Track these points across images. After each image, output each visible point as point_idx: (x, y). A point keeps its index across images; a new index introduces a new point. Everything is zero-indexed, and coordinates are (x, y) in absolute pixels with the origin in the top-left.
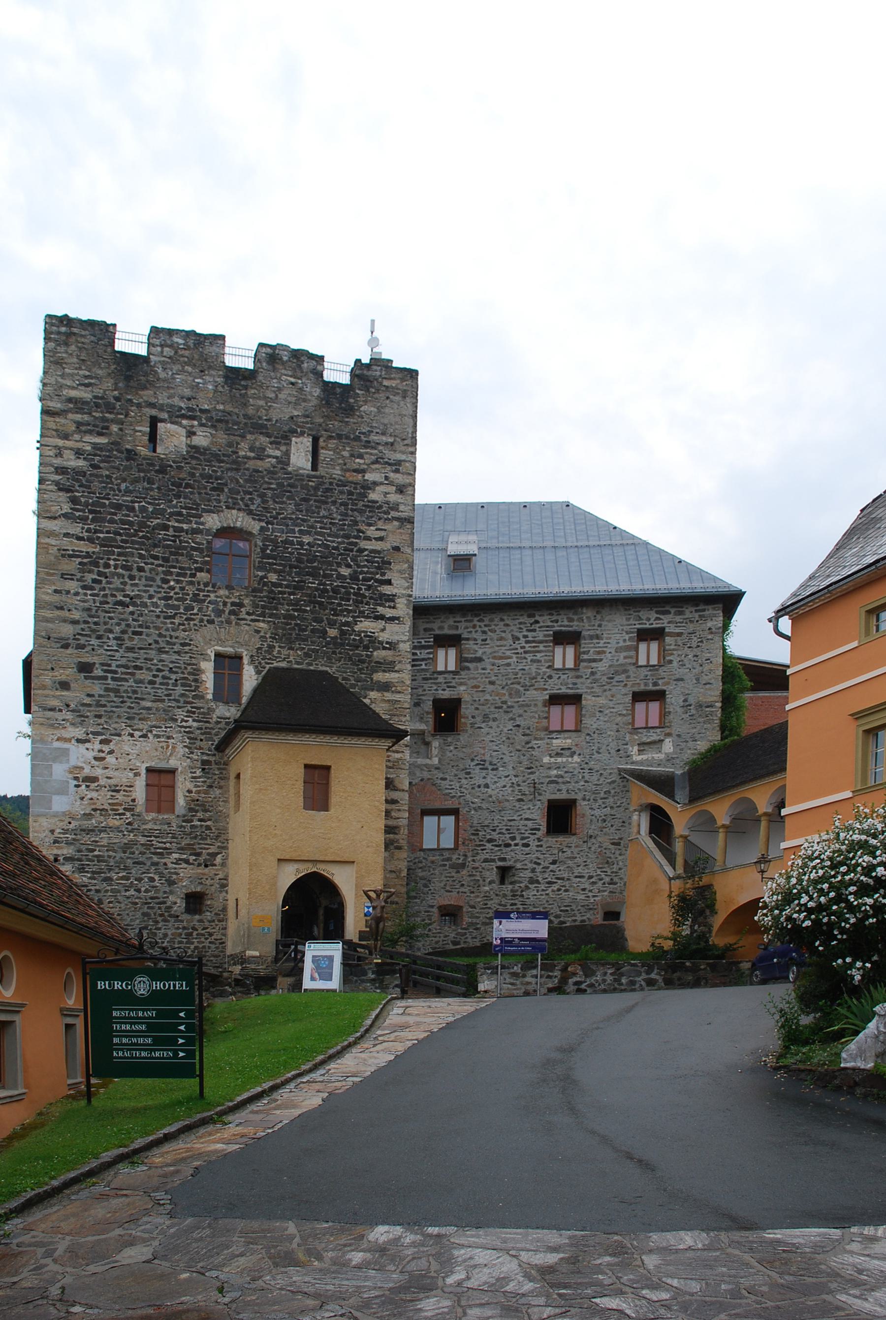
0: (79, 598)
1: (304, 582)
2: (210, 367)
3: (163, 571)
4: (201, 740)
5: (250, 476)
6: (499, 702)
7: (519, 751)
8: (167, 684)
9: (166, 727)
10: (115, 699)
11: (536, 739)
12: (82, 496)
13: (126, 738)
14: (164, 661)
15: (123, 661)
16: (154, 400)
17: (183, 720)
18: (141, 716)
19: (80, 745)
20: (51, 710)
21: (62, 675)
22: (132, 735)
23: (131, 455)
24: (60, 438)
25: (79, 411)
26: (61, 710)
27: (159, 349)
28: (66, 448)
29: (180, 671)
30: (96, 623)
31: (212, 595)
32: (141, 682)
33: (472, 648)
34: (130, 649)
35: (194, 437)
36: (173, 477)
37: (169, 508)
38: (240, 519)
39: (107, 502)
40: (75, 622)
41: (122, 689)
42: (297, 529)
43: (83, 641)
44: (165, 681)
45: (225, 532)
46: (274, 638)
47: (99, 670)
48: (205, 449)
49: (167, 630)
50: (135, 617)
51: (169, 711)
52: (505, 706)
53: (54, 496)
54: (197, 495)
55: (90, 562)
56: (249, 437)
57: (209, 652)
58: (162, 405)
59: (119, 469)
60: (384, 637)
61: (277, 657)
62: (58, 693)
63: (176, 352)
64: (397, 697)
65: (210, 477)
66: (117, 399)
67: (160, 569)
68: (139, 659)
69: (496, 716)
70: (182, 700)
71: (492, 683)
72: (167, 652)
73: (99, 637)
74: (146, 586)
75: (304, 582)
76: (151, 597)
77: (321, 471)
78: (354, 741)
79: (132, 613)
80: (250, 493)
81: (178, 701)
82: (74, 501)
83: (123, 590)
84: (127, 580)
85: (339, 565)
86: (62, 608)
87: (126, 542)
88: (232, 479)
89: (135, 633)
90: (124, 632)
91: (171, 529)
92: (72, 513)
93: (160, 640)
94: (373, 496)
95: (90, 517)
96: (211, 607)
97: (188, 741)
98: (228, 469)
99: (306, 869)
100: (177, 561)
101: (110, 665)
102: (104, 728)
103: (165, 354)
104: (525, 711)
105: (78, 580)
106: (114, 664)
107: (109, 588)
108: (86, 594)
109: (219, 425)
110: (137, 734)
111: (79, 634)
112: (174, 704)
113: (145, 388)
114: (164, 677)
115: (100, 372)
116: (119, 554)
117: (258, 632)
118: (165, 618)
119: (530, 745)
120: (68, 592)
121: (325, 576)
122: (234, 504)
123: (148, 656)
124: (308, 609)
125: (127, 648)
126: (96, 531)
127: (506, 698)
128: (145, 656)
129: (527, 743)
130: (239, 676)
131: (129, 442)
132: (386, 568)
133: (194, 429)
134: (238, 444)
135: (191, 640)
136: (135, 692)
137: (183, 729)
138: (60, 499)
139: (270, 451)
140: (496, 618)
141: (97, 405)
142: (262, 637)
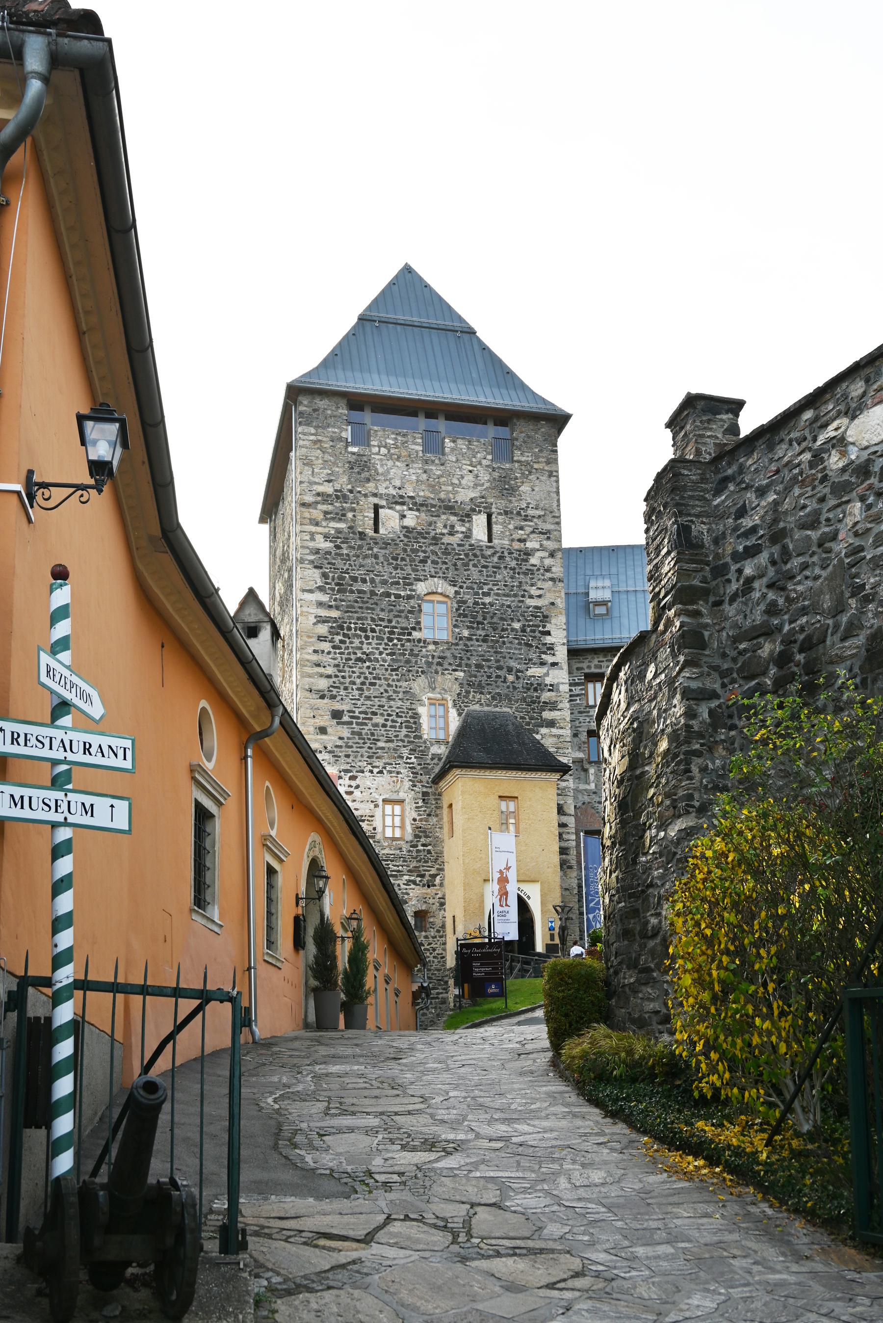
2: (413, 461)
3: (389, 632)
5: (446, 549)
8: (395, 727)
13: (368, 774)
15: (363, 708)
17: (407, 758)
22: (371, 772)
23: (362, 536)
24: (313, 525)
25: (325, 502)
27: (377, 449)
30: (343, 677)
31: (424, 650)
32: (376, 725)
34: (368, 698)
35: (405, 520)
37: (390, 578)
40: (329, 677)
41: (364, 732)
42: (480, 591)
46: (469, 685)
49: (393, 680)
50: (370, 670)
55: (338, 627)
56: (444, 517)
57: (423, 698)
58: (381, 494)
59: (354, 548)
60: (548, 681)
62: (319, 737)
63: (389, 451)
64: (560, 732)
65: (418, 551)
66: (351, 491)
67: (386, 629)
70: (406, 740)
72: (394, 700)
73: (346, 689)
74: (377, 644)
75: (488, 636)
76: (381, 653)
77: (496, 542)
78: (533, 775)
79: (368, 667)
80: (446, 563)
82: (325, 576)
83: (361, 648)
84: (364, 640)
85: (512, 620)
86: (318, 665)
87: (361, 608)
90: (363, 683)
91: (393, 597)
93: (389, 689)
94: (533, 560)
96: (424, 659)
100: (398, 622)
101: (354, 712)
105: (330, 642)
106: (357, 710)
108: (335, 653)
110: (376, 770)
111: (332, 686)
112: (400, 744)
113: (368, 480)
114: (393, 721)
115: (337, 469)
116: (358, 619)
117: (456, 679)
118: (392, 670)
120: (323, 652)
121: (503, 630)
123: (381, 703)
125: (366, 697)
130: (446, 717)
133: (405, 513)
136: (373, 734)
139: (458, 528)
141: (337, 497)
142: (461, 684)
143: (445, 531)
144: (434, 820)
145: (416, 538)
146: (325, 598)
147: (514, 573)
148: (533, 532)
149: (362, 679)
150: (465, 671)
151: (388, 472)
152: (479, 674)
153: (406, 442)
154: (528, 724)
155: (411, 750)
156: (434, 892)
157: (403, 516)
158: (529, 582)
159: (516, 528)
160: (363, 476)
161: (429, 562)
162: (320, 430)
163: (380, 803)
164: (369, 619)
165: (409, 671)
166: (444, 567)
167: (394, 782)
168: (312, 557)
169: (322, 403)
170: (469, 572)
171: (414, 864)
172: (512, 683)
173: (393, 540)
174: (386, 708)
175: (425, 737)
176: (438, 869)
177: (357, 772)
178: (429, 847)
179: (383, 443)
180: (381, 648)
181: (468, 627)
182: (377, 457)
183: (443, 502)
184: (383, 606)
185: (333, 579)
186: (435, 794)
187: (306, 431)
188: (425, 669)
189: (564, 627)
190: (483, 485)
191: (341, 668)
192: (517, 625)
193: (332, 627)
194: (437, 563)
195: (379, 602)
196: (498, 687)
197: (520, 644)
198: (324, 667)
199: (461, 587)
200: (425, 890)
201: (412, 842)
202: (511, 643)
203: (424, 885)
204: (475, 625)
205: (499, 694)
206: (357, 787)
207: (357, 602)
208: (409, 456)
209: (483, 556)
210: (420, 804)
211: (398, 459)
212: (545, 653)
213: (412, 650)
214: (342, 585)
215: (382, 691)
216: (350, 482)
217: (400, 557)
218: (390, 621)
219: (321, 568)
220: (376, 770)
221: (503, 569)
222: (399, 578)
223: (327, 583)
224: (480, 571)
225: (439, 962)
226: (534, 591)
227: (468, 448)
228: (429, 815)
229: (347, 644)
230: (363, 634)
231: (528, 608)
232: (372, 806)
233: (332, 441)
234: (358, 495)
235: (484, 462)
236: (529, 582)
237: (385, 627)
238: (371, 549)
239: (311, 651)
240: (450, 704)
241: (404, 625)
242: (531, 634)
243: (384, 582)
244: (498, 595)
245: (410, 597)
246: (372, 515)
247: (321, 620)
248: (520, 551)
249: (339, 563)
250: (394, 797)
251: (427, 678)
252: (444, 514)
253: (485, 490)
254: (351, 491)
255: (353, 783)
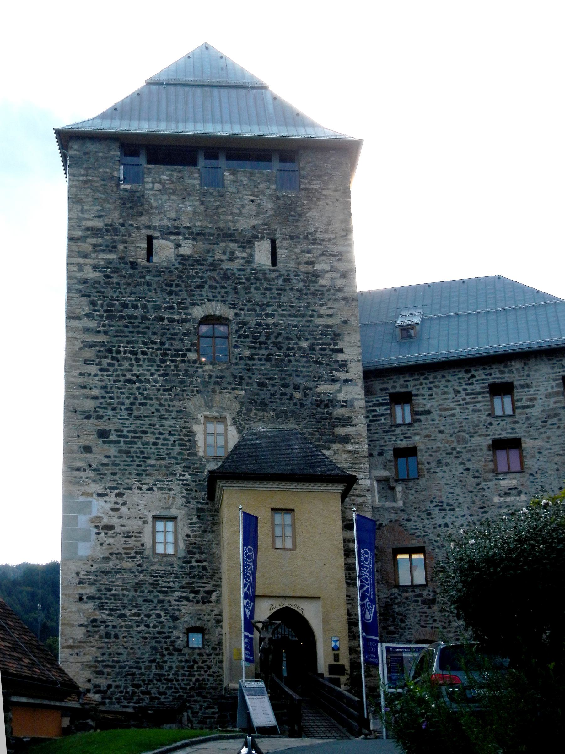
0: (97, 378)
1: (272, 355)
2: (189, 195)
3: (161, 354)
4: (196, 491)
5: (225, 274)
6: (449, 448)
7: (471, 492)
8: (167, 445)
9: (167, 481)
10: (127, 459)
11: (485, 480)
12: (98, 300)
13: (136, 491)
14: (164, 426)
15: (132, 427)
16: (148, 223)
17: (180, 475)
18: (147, 472)
19: (100, 498)
20: (78, 469)
21: (84, 441)
22: (140, 489)
23: (134, 265)
25: (95, 235)
26: (84, 470)
27: (151, 185)
28: (86, 265)
29: (177, 433)
30: (111, 398)
31: (200, 370)
32: (147, 443)
33: (422, 403)
34: (138, 418)
35: (180, 248)
36: (165, 280)
37: (164, 304)
38: (218, 308)
39: (117, 303)
40: (95, 398)
41: (132, 450)
42: (263, 313)
43: (101, 412)
44: (166, 442)
45: (207, 320)
46: (251, 403)
47: (114, 436)
48: (189, 257)
49: (166, 400)
50: (141, 391)
51: (170, 467)
52: (454, 452)
53: (77, 301)
54: (184, 292)
56: (222, 244)
57: (199, 416)
59: (125, 277)
60: (341, 397)
61: (254, 418)
62: (83, 455)
63: (164, 186)
65: (194, 277)
66: (123, 225)
67: (159, 352)
68: (145, 425)
69: (448, 461)
70: (179, 457)
71: (441, 432)
72: (166, 419)
73: (114, 409)
74: (148, 366)
75: (272, 355)
76: (152, 374)
77: (280, 265)
79: (139, 388)
80: (225, 288)
81: (176, 458)
82: (93, 303)
83: (131, 370)
84: (134, 362)
85: (299, 339)
86: (85, 387)
87: (130, 332)
88: (211, 278)
89: (142, 404)
90: (132, 404)
92: (91, 313)
95: (105, 315)
97: (185, 492)
98: (207, 271)
99: (278, 605)
100: (171, 344)
101: (122, 431)
102: (118, 484)
103: (155, 188)
104: (473, 456)
105: (97, 365)
106: (125, 430)
107: (121, 370)
109: (199, 238)
110: (145, 487)
112: (173, 461)
113: (141, 214)
114: (165, 439)
115: (108, 206)
116: (128, 342)
117: (236, 398)
118: (164, 390)
119: (480, 486)
120: (89, 374)
121: (288, 349)
122: (213, 297)
123: (152, 422)
124: (277, 376)
125: (135, 417)
126: (110, 326)
127: (455, 445)
128: (150, 422)
129: (478, 484)
131: (132, 256)
132: (340, 340)
133: (180, 243)
134: (213, 250)
135: (185, 408)
136: (142, 452)
137: (181, 482)
138: (82, 303)
139: (238, 254)
140: (439, 374)
141: (108, 231)
143: (224, 257)
144: (209, 536)
145: (192, 265)
146: (92, 324)
147: (302, 294)
148: (323, 254)
149: (132, 400)
150: (245, 390)
151: (162, 205)
152: (261, 392)
153: (182, 177)
154: (319, 440)
155: (185, 467)
156: (210, 608)
157: (178, 246)
158: (318, 302)
159: (303, 251)
160: (135, 210)
161: (206, 286)
162: (90, 171)
163: (150, 520)
164: (140, 342)
165: (183, 391)
166: (223, 291)
167: (165, 498)
168: (80, 287)
169: (92, 147)
170: (251, 295)
171: (188, 580)
172: (299, 400)
173: (167, 268)
174: (157, 426)
175: (201, 454)
176: (214, 585)
177: (124, 489)
178: (205, 564)
179: (158, 180)
180: (153, 369)
181: (250, 347)
182: (151, 192)
183: (222, 230)
184: (155, 330)
185: (102, 306)
186: (211, 510)
187: (76, 172)
188: (201, 388)
189: (359, 344)
190: (266, 212)
191: (109, 389)
192: (304, 344)
193: (99, 351)
194: (216, 288)
195: (151, 326)
196: (283, 404)
197: (308, 362)
198: (91, 389)
199: (242, 309)
200: (199, 607)
201: (184, 558)
202: (298, 361)
203: (198, 602)
204: (257, 345)
205: (286, 412)
206: (124, 504)
207: (127, 327)
208: (186, 190)
209: (266, 280)
210: (195, 520)
211: (173, 193)
212: (336, 370)
213: (186, 371)
214: (112, 311)
215: (153, 410)
216: (121, 216)
217: (174, 283)
218: (163, 344)
219: (89, 296)
220: (145, 487)
221: (288, 291)
222: (173, 303)
223: (95, 310)
224: (262, 294)
225: (215, 680)
226: (324, 311)
227: (250, 180)
228: (205, 531)
229: (116, 367)
230: (133, 357)
231: (318, 327)
232: (140, 522)
233: (103, 180)
234: (130, 228)
235: (268, 192)
236: (318, 302)
237: (157, 349)
238: (144, 277)
239: (76, 374)
240: (229, 422)
241: (178, 347)
242: (321, 352)
243: (157, 308)
244: (282, 315)
245: (184, 321)
246: (145, 246)
247: (88, 345)
248: (307, 273)
249: (109, 292)
250: (165, 513)
251: (203, 397)
252: (223, 241)
253: (268, 217)
254: (123, 225)
255: (120, 500)
